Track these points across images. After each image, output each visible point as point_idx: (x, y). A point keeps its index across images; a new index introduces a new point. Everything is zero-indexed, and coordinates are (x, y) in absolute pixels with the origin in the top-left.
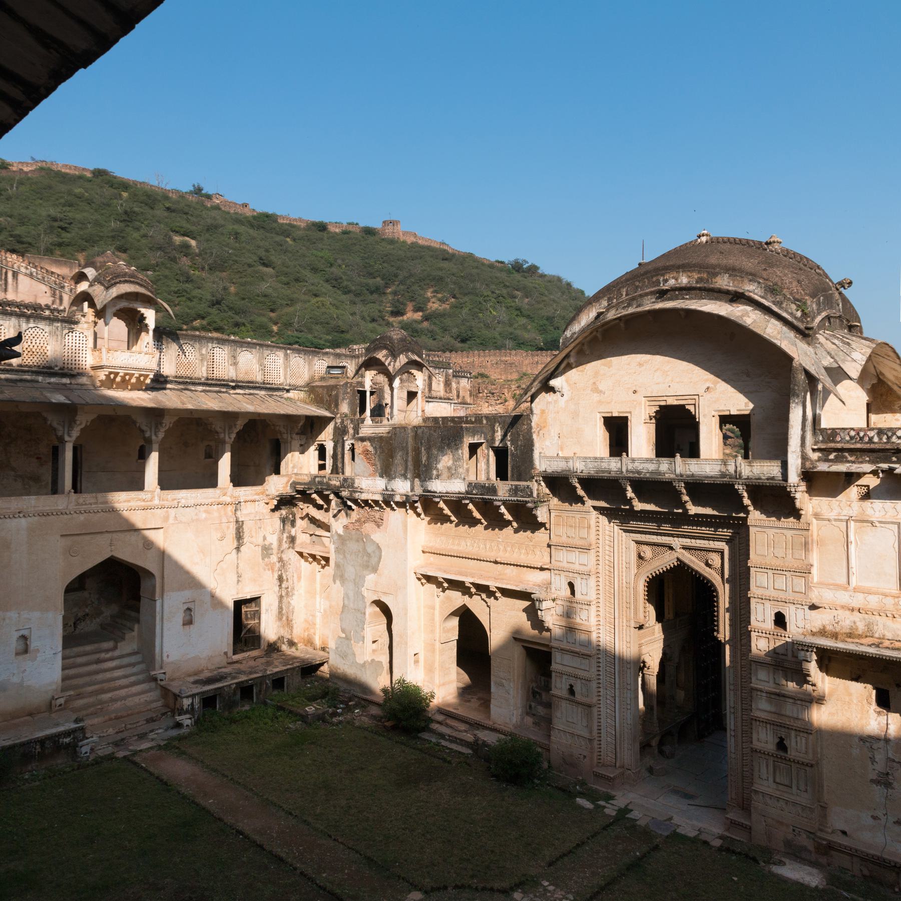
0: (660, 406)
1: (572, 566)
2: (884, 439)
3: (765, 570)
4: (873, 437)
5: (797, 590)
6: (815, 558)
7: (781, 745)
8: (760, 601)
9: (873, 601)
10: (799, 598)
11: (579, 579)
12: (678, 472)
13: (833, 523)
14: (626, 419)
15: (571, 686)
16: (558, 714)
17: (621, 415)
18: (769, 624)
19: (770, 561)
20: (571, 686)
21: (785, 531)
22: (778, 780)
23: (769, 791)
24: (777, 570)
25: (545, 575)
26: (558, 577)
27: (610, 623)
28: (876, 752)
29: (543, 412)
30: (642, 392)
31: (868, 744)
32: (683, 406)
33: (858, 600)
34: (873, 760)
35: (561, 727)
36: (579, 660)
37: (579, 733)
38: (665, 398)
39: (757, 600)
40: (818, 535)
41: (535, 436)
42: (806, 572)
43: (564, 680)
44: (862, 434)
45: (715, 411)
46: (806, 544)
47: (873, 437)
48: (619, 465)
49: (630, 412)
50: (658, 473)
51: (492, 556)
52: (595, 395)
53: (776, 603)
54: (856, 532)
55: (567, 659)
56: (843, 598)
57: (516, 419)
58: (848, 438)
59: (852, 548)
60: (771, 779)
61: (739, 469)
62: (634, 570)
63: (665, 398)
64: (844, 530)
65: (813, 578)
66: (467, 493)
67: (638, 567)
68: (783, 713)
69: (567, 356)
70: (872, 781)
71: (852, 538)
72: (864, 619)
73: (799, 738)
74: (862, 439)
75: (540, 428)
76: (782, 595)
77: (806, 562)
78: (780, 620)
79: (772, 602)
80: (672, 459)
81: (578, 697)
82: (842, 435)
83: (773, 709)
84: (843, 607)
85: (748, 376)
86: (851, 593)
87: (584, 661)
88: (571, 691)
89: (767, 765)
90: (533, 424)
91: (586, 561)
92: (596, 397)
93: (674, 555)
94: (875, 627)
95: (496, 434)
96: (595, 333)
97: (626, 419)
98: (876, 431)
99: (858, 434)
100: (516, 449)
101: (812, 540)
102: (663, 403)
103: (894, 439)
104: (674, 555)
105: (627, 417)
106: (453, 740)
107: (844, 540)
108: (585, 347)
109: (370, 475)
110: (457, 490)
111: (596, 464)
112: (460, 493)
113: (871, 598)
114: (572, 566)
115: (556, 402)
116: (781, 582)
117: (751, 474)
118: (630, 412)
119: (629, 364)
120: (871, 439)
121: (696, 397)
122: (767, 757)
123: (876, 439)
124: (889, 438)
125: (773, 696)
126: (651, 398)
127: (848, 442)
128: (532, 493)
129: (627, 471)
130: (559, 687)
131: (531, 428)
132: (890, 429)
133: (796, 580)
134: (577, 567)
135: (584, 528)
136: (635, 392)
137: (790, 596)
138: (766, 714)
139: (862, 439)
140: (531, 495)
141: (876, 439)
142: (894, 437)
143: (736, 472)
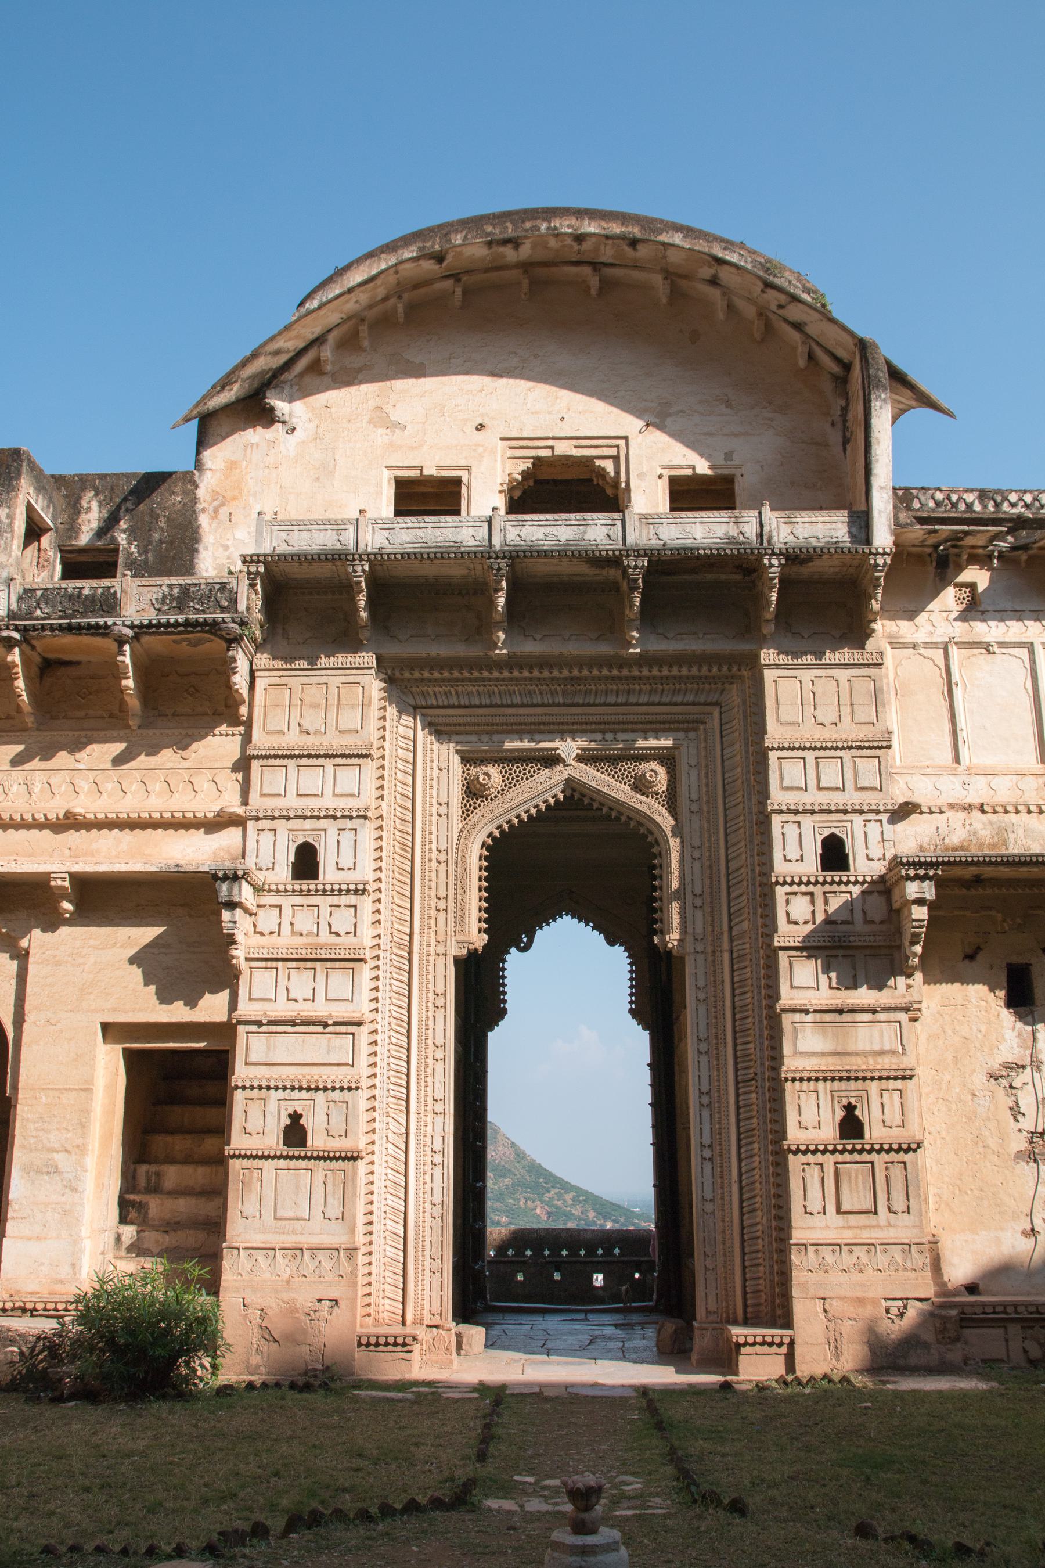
0: (538, 461)
2: (991, 507)
3: (800, 753)
4: (972, 503)
6: (893, 718)
8: (791, 817)
9: (1004, 791)
10: (871, 799)
11: (333, 833)
13: (922, 651)
14: (457, 482)
15: (295, 1117)
16: (250, 1207)
18: (811, 866)
19: (809, 733)
20: (295, 1117)
21: (835, 672)
22: (846, 1206)
23: (830, 1236)
25: (231, 837)
27: (400, 946)
28: (1019, 1093)
29: (232, 465)
31: (1004, 1082)
33: (978, 791)
34: (1016, 1112)
35: (790, 799)
37: (315, 1241)
38: (550, 443)
39: (784, 817)
40: (896, 675)
41: (203, 520)
43: (272, 1106)
45: (663, 467)
46: (877, 692)
47: (972, 503)
49: (468, 469)
51: (55, 808)
52: (381, 431)
53: (825, 817)
54: (961, 665)
55: (288, 1047)
56: (952, 789)
57: (151, 483)
58: (932, 504)
59: (958, 693)
60: (831, 1208)
61: (766, 529)
62: (457, 823)
63: (550, 443)
64: (941, 663)
65: (894, 758)
67: (466, 813)
68: (851, 1048)
69: (318, 341)
71: (956, 676)
72: (991, 823)
74: (954, 505)
75: (221, 500)
76: (838, 799)
77: (879, 727)
78: (834, 854)
79: (817, 817)
81: (317, 1141)
82: (923, 499)
83: (828, 1046)
84: (952, 806)
85: (728, 404)
90: (201, 493)
91: (355, 784)
92: (381, 436)
93: (559, 774)
94: (1012, 836)
95: (83, 517)
96: (393, 301)
97: (457, 482)
98: (976, 494)
99: (948, 498)
100: (143, 550)
101: (888, 684)
102: (545, 453)
103: (1006, 507)
104: (559, 774)
107: (941, 683)
108: (364, 329)
113: (997, 782)
115: (273, 442)
116: (831, 773)
117: (791, 538)
118: (468, 469)
120: (969, 506)
121: (622, 443)
123: (977, 507)
124: (997, 505)
125: (828, 1017)
127: (933, 510)
131: (195, 500)
132: (999, 492)
133: (863, 765)
134: (328, 803)
135: (353, 706)
136: (480, 427)
137: (852, 797)
139: (954, 505)
141: (977, 507)
142: (1006, 504)
143: (760, 535)
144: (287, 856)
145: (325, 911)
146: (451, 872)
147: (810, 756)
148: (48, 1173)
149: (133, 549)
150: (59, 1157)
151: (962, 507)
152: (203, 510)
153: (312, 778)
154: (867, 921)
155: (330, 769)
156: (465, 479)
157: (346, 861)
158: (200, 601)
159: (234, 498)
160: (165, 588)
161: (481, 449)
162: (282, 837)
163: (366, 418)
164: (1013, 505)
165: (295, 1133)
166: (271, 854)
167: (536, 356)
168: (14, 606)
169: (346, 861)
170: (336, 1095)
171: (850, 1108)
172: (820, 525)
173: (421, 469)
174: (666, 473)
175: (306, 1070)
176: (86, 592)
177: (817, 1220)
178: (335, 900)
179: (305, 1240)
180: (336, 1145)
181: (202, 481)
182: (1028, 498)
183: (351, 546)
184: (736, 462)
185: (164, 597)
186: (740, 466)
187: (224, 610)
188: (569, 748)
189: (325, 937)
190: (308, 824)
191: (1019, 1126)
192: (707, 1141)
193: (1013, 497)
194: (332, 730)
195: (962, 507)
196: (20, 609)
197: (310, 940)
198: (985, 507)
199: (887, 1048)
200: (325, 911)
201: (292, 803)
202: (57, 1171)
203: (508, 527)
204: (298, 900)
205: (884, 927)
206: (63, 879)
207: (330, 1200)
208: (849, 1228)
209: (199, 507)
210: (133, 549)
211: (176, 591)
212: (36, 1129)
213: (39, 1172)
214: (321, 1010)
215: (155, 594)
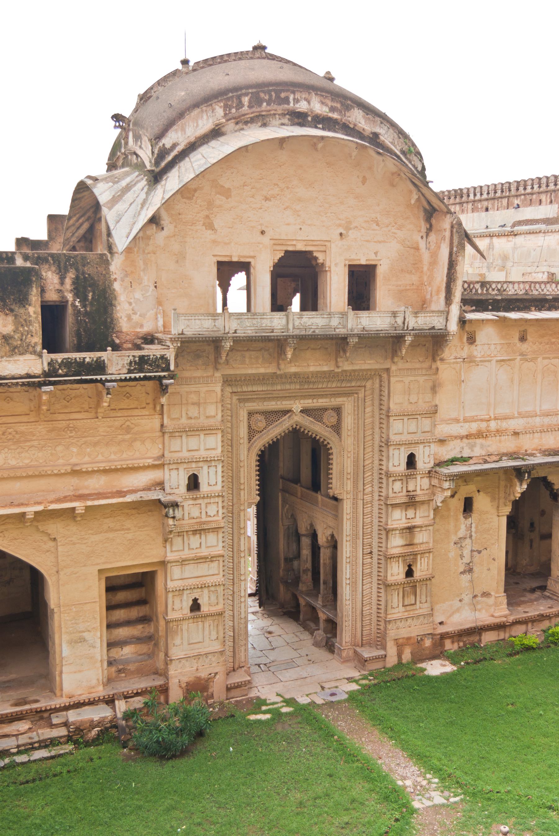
0: (286, 252)
1: (196, 454)
5: (426, 430)
7: (409, 573)
10: (428, 436)
11: (205, 468)
12: (350, 326)
13: (452, 365)
15: (195, 600)
16: (177, 641)
17: (242, 260)
20: (195, 600)
24: (411, 416)
26: (174, 473)
30: (270, 233)
31: (459, 545)
32: (311, 252)
34: (462, 556)
36: (206, 565)
38: (294, 243)
42: (434, 411)
44: (472, 286)
48: (284, 321)
49: (253, 257)
50: (328, 326)
60: (401, 605)
66: (46, 374)
70: (461, 573)
73: (423, 559)
74: (471, 291)
76: (415, 438)
80: (284, 313)
84: (456, 437)
86: (462, 424)
87: (215, 564)
88: (196, 606)
89: (398, 594)
98: (480, 284)
99: (469, 286)
102: (291, 249)
105: (249, 263)
106: (31, 748)
109: (6, 355)
110: (23, 372)
111: (255, 322)
112: (28, 376)
114: (196, 454)
119: (253, 197)
122: (425, 583)
124: (487, 290)
126: (277, 242)
128: (168, 365)
129: (294, 328)
130: (176, 608)
134: (203, 453)
138: (399, 549)
140: (167, 369)
144: (184, 482)
145: (203, 506)
146: (246, 470)
147: (406, 419)
148: (81, 642)
149: (77, 304)
150: (85, 635)
151: (474, 291)
152: (115, 280)
153: (193, 442)
154: (421, 490)
155: (202, 436)
156: (252, 264)
157: (213, 482)
158: (151, 365)
159: (132, 272)
160: (131, 358)
161: (261, 246)
162: (181, 471)
163: (201, 223)
164: (493, 290)
165: (196, 606)
166: (177, 481)
167: (288, 188)
168: (46, 369)
169: (213, 482)
170: (212, 589)
171: (410, 566)
172: (428, 318)
173: (231, 257)
174: (347, 263)
175: (199, 579)
176: (87, 360)
177: (396, 611)
178: (207, 501)
179: (204, 651)
180: (214, 609)
181: (113, 260)
182: (499, 286)
183: (222, 328)
184: (378, 258)
185: (131, 363)
186: (380, 260)
187: (163, 371)
188: (297, 406)
189: (204, 518)
190: (194, 465)
191: (463, 561)
192: (348, 577)
193: (494, 286)
194: (202, 418)
195: (474, 291)
196: (49, 370)
197: (198, 520)
198: (482, 290)
199: (425, 541)
200: (203, 506)
201: (185, 454)
202: (85, 640)
203: (296, 319)
204: (191, 502)
205: (427, 492)
206: (82, 510)
207: (212, 633)
208: (406, 611)
209: (113, 277)
210: (77, 304)
211: (137, 359)
212: (72, 624)
213: (76, 642)
214: (204, 552)
215: (127, 361)
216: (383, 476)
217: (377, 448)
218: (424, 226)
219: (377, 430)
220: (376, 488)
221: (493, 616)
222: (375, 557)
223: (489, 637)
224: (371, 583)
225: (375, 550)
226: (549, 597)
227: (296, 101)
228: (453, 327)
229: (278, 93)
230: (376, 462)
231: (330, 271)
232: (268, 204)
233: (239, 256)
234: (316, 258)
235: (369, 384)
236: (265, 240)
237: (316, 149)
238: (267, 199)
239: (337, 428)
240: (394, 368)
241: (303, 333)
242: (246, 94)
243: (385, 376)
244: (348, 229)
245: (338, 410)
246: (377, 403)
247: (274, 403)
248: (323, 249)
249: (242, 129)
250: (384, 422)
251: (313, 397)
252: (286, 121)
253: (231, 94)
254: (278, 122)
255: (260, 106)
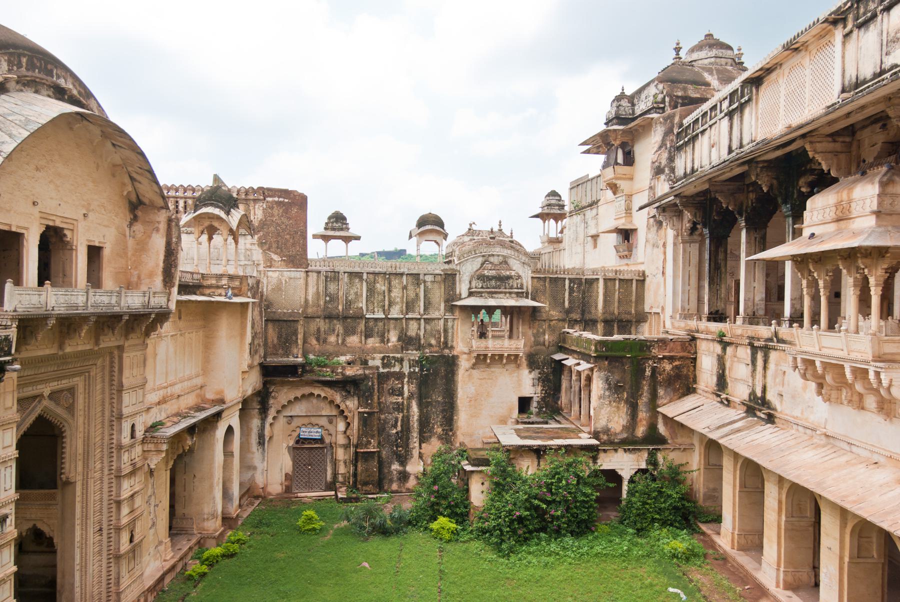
32: (63, 229)
38: (54, 218)
49: (27, 229)
102: (51, 224)
111: (66, 297)
126: (44, 215)
187: (5, 355)
216: (113, 450)
217: (107, 423)
218: (129, 217)
219: (107, 405)
220: (106, 464)
221: (165, 561)
222: (105, 532)
223: (168, 580)
224: (101, 561)
225: (105, 526)
226: (177, 534)
227: (58, 77)
228: (173, 306)
229: (46, 63)
230: (106, 438)
231: (76, 250)
232: (38, 174)
233: (18, 227)
234: (65, 235)
235: (99, 362)
236: (36, 211)
237: (71, 129)
238: (37, 169)
239: (71, 409)
240: (126, 345)
241: (104, 310)
242: (25, 55)
243: (116, 352)
244: (89, 210)
245: (72, 390)
246: (107, 379)
247: (30, 388)
248: (71, 227)
249: (22, 91)
250: (115, 396)
251: (59, 379)
252: (51, 94)
253: (11, 50)
254: (46, 93)
255: (34, 71)
